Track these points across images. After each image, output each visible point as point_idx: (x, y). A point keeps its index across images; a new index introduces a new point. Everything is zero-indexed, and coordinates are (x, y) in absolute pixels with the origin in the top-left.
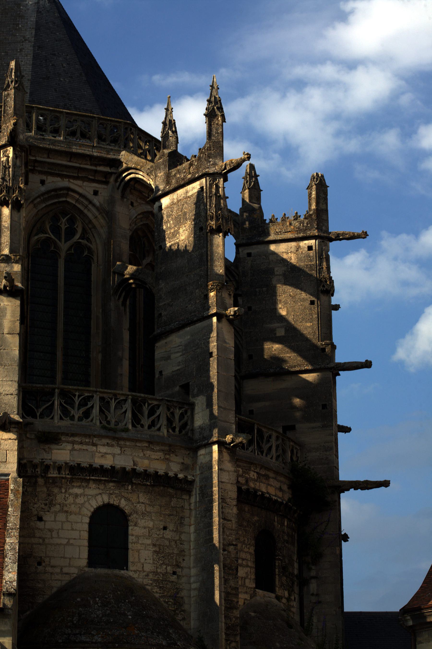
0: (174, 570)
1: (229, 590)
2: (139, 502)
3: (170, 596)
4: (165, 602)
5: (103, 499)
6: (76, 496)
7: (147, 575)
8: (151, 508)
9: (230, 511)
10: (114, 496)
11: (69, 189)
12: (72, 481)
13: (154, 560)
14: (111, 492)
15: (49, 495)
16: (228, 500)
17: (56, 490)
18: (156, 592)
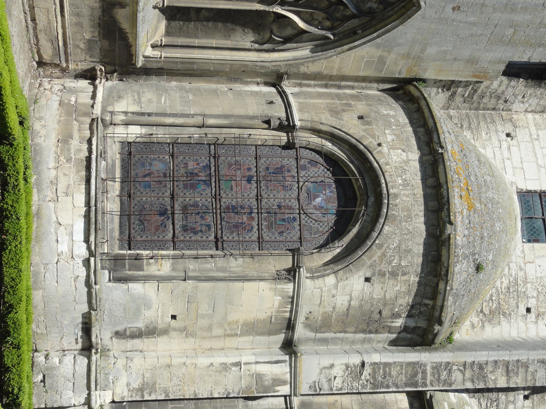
0: (532, 310)
1: (531, 369)
3: (499, 303)
4: (492, 296)
7: (521, 269)
13: (541, 278)
18: (502, 282)
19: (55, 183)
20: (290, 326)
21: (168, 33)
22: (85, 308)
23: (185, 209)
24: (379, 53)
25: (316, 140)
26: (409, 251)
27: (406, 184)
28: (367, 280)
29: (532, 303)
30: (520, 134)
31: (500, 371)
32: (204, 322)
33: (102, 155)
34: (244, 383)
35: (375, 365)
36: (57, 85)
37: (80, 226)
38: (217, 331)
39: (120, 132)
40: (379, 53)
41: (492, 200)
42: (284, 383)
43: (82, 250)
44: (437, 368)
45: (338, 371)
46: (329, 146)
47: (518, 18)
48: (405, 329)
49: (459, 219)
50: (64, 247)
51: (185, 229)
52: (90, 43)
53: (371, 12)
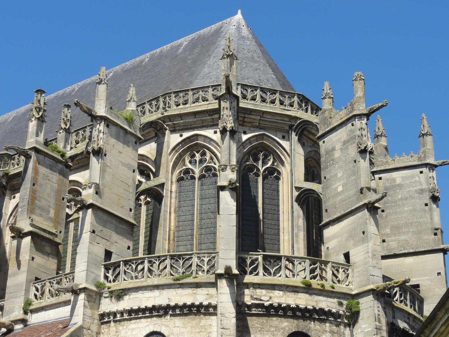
2: (175, 327)
5: (149, 329)
6: (133, 329)
8: (184, 329)
9: (228, 322)
10: (157, 325)
11: (197, 135)
12: (130, 319)
14: (155, 323)
15: (117, 332)
16: (227, 315)
17: (121, 328)
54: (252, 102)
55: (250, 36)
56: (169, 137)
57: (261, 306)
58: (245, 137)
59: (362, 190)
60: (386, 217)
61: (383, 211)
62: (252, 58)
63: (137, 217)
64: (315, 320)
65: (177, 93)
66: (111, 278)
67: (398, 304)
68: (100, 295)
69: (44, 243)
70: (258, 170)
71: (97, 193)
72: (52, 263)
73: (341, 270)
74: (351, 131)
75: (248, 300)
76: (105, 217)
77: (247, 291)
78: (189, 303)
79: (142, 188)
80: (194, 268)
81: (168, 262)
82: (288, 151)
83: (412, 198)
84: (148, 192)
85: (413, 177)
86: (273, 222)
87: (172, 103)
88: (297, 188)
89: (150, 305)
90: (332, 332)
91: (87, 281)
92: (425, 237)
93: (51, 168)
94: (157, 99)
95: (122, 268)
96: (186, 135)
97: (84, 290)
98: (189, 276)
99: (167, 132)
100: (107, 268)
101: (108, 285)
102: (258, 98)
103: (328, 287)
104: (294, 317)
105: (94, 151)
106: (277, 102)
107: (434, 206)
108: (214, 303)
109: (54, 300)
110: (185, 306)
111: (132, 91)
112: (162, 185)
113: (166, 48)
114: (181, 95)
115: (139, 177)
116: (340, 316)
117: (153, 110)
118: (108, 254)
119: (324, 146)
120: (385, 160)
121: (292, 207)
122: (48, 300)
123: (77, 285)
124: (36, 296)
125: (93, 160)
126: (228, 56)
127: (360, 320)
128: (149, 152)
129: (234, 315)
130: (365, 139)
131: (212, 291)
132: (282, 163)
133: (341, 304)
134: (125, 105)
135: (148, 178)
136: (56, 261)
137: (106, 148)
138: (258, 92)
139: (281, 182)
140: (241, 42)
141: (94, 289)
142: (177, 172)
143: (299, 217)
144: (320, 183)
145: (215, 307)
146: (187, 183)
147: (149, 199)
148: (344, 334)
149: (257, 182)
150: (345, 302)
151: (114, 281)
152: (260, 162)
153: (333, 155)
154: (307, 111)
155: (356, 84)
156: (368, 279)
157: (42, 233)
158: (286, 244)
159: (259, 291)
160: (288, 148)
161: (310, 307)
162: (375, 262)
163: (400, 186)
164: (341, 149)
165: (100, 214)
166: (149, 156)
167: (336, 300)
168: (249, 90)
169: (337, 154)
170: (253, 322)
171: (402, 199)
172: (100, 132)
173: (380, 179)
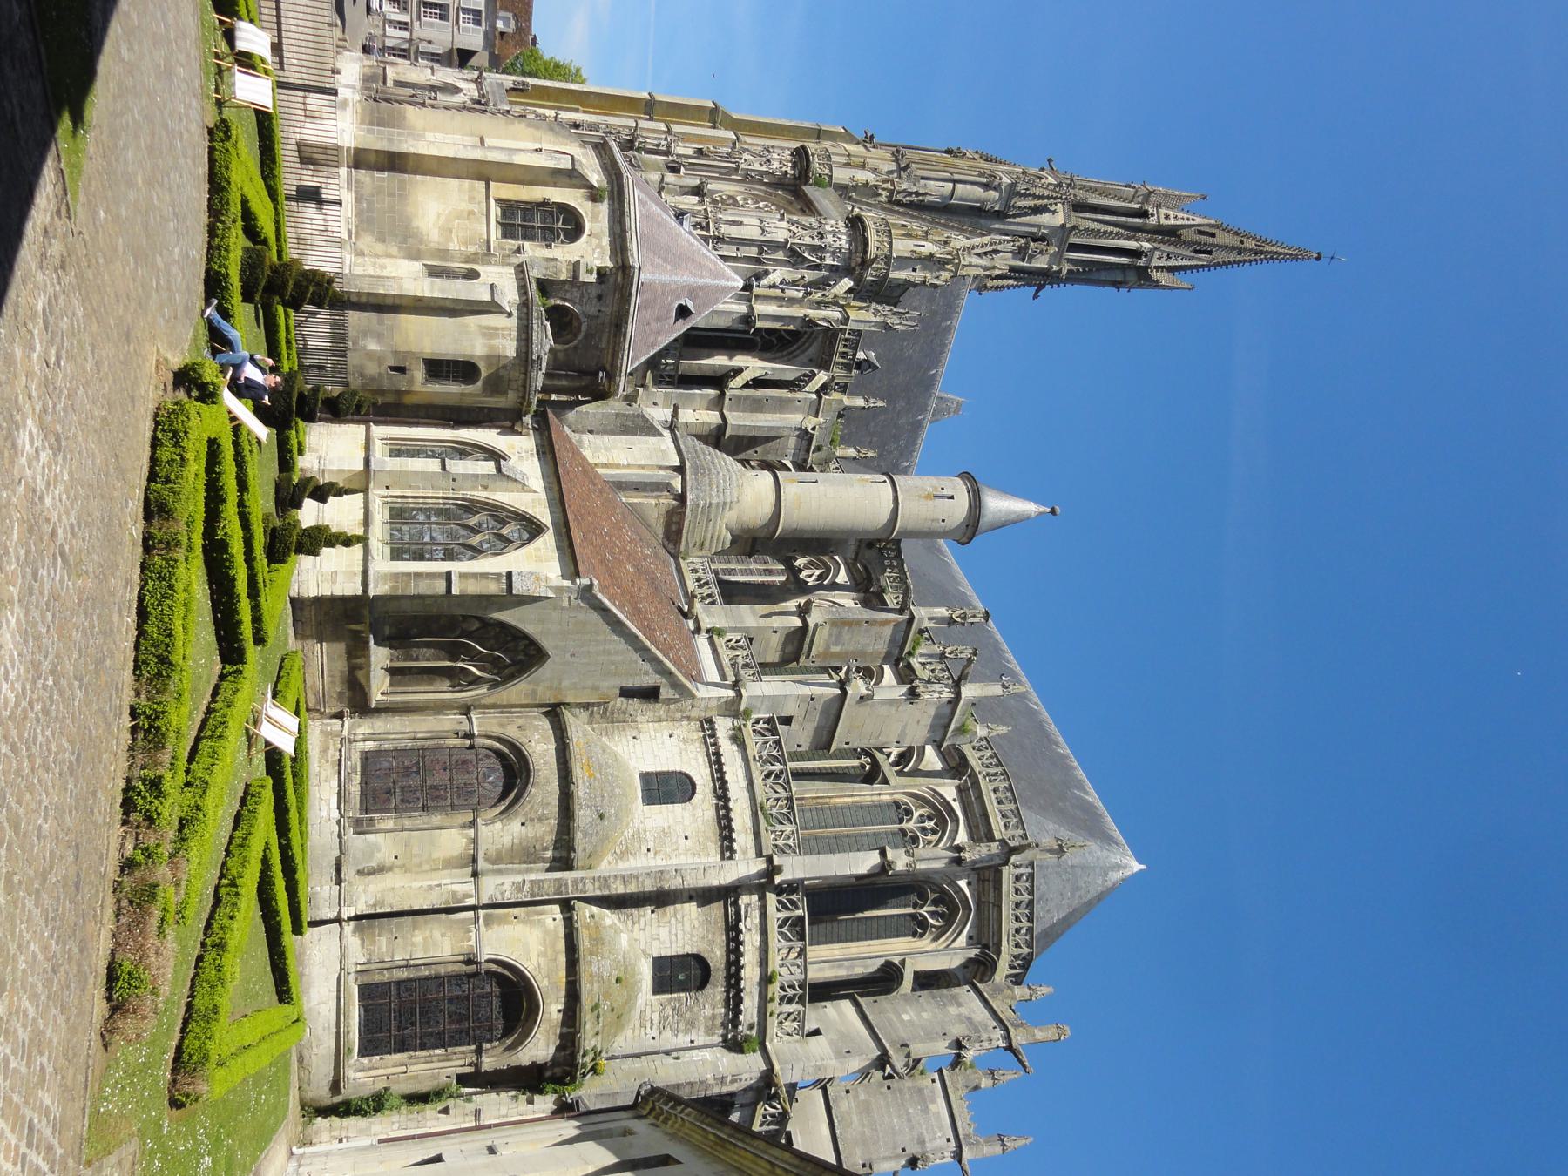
12: (708, 755)
17: (697, 745)
19: (318, 775)
20: (474, 860)
21: (391, 685)
22: (337, 853)
23: (402, 789)
24: (531, 687)
25: (489, 742)
26: (548, 804)
27: (545, 763)
28: (523, 824)
29: (651, 845)
30: (642, 737)
31: (619, 881)
32: (416, 861)
33: (348, 758)
34: (443, 898)
35: (532, 882)
36: (318, 723)
37: (334, 799)
38: (426, 867)
39: (360, 746)
40: (531, 687)
41: (612, 775)
42: (471, 896)
43: (336, 814)
44: (575, 882)
45: (507, 887)
46: (498, 745)
47: (614, 658)
48: (554, 859)
49: (580, 781)
50: (324, 814)
51: (403, 801)
52: (340, 694)
53: (520, 662)
54: (1012, 890)
55: (1109, 884)
56: (951, 784)
57: (738, 919)
58: (962, 884)
59: (906, 1045)
60: (881, 1093)
61: (889, 1088)
62: (1078, 888)
63: (841, 754)
64: (727, 992)
65: (1010, 789)
66: (757, 727)
67: (760, 1111)
68: (736, 716)
69: (796, 643)
70: (922, 907)
71: (861, 698)
72: (773, 656)
73: (795, 1024)
74: (986, 1028)
75: (744, 900)
76: (834, 711)
77: (755, 897)
78: (734, 825)
79: (879, 756)
80: (779, 827)
81: (784, 794)
82: (953, 945)
83: (912, 1128)
84: (875, 764)
85: (941, 1128)
86: (855, 933)
87: (995, 784)
88: (903, 962)
89: (727, 777)
90: (713, 1017)
91: (750, 697)
92: (858, 1152)
93: (892, 641)
94: (999, 764)
95: (771, 739)
96: (957, 807)
97: (740, 695)
98: (768, 822)
99: (957, 781)
100: (769, 721)
101: (749, 724)
102: (1019, 898)
103: (772, 1007)
104: (729, 964)
105: (915, 687)
106: (1018, 925)
107: (903, 1162)
108: (737, 856)
109: (726, 662)
110: (730, 820)
111: (1002, 730)
112: (885, 781)
113: (1081, 774)
114: (1009, 794)
115: (895, 752)
116: (735, 1027)
117: (984, 761)
118: (787, 721)
119: (964, 992)
120: (960, 1086)
121: (877, 957)
122: (726, 656)
123: (744, 686)
124: (730, 640)
125: (904, 689)
126: (1061, 846)
127: (732, 1054)
128: (929, 761)
129: (723, 883)
130: (977, 1046)
131: (752, 852)
132: (936, 939)
133: (751, 1027)
134: (984, 721)
135: (896, 764)
136: (776, 660)
137: (920, 703)
138: (1026, 897)
139: (910, 938)
140: (1098, 870)
141: (742, 708)
142: (906, 799)
143: (866, 967)
144: (914, 990)
145: (731, 858)
146: (893, 813)
147: (868, 767)
148: (713, 1034)
149: (906, 906)
150: (754, 1033)
151: (754, 731)
152: (933, 909)
153: (952, 1005)
154: (1012, 967)
155: (1053, 1029)
156: (786, 1063)
157: (808, 640)
158: (828, 953)
159: (757, 914)
160: (955, 945)
161: (742, 984)
162: (811, 1070)
163: (926, 1111)
164: (960, 1015)
165: (836, 706)
166: (923, 763)
167: (756, 1020)
168: (1027, 884)
169: (953, 1010)
170: (716, 909)
171: (908, 1114)
172: (940, 693)
173: (933, 1081)
